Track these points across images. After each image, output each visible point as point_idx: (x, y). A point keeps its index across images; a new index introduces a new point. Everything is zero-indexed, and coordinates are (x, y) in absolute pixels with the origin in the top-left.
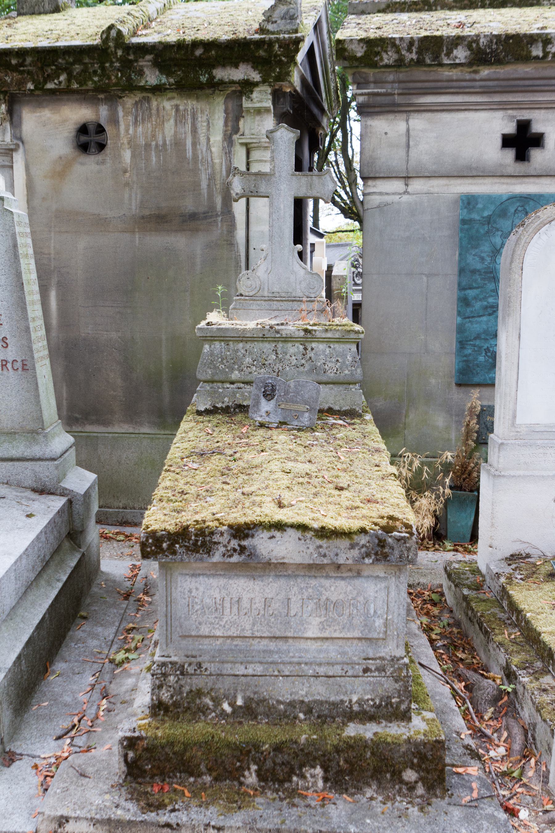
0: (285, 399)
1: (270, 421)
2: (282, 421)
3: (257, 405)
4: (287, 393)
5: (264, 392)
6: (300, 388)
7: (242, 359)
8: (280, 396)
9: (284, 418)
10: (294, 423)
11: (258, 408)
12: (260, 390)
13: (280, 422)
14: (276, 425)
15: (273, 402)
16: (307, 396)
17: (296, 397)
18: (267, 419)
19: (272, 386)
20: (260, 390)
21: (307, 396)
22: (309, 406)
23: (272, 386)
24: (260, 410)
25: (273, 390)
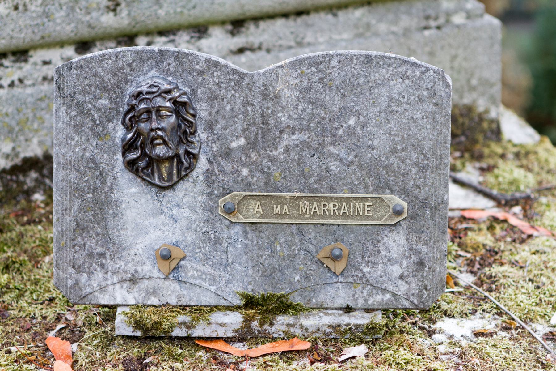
0: (255, 167)
1: (192, 297)
2: (259, 292)
3: (102, 220)
4: (262, 134)
5: (128, 147)
6: (334, 101)
7: (249, 175)
8: (227, 154)
9: (268, 275)
10: (326, 296)
11: (106, 238)
12: (99, 133)
13: (250, 302)
14: (234, 320)
15: (189, 194)
16: (380, 140)
17: (319, 151)
18: (173, 292)
19: (179, 107)
20: (99, 133)
21: (380, 140)
22: (404, 193)
23: (179, 107)
24: (119, 250)
25: (184, 131)
